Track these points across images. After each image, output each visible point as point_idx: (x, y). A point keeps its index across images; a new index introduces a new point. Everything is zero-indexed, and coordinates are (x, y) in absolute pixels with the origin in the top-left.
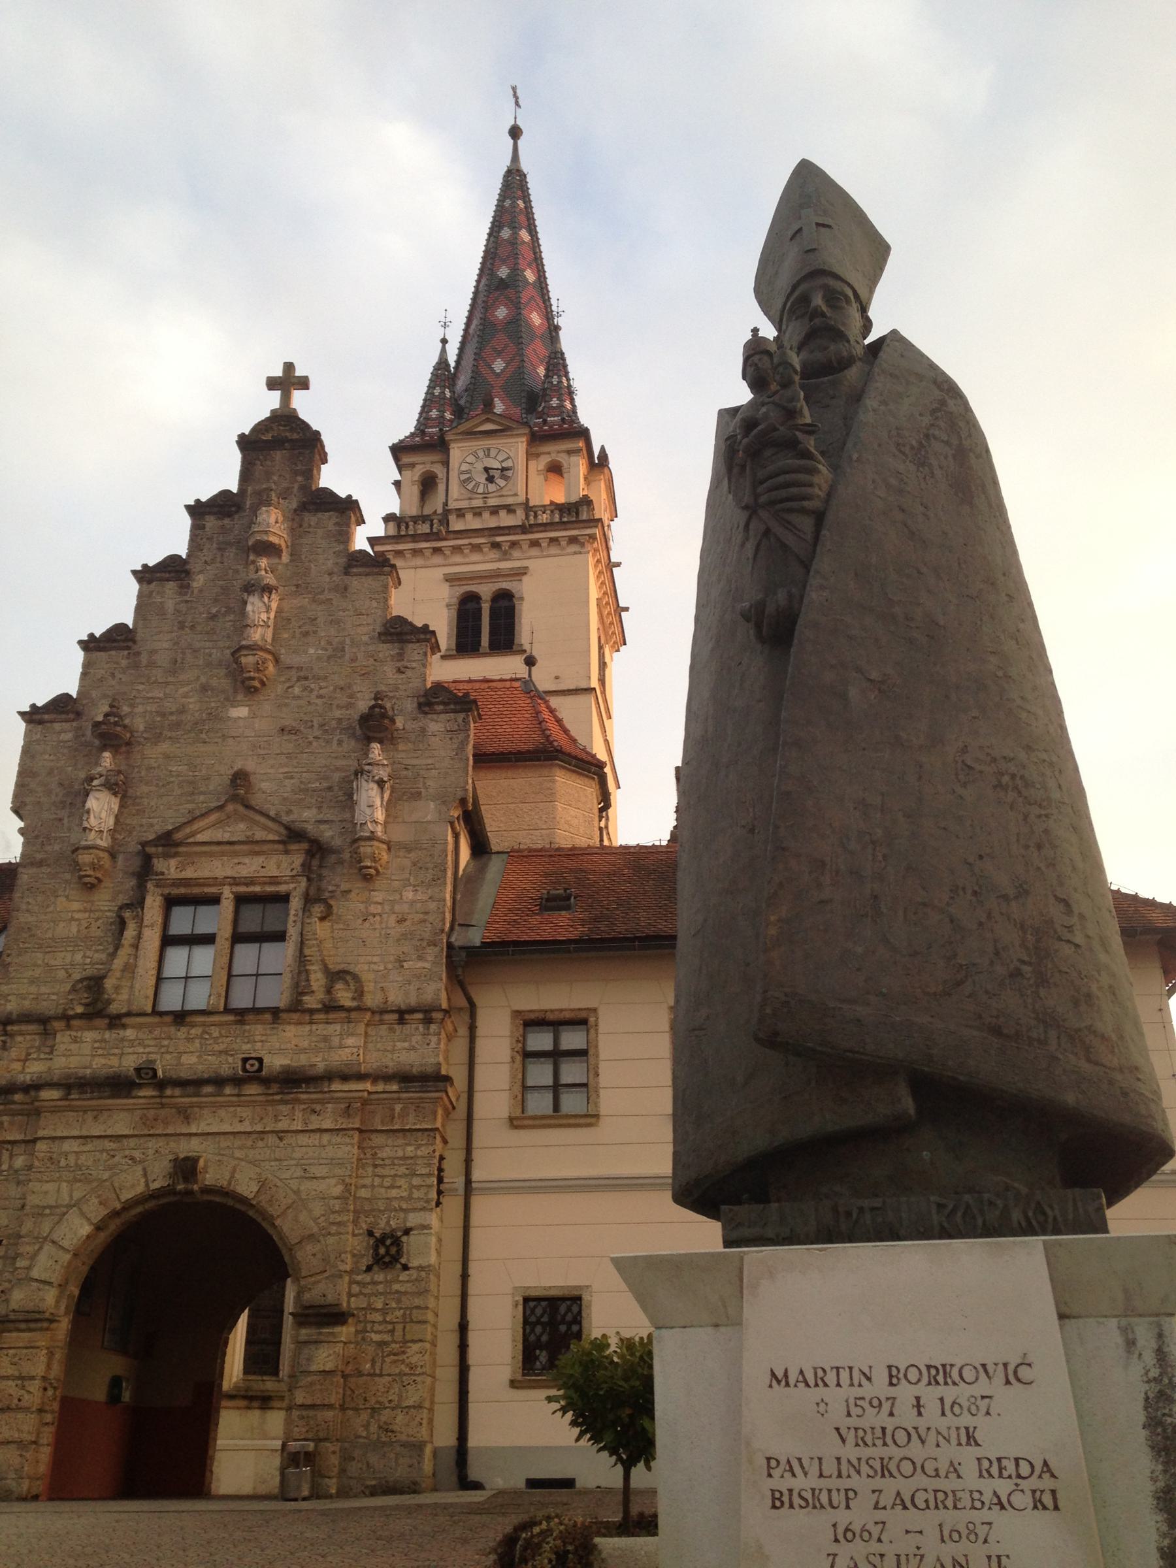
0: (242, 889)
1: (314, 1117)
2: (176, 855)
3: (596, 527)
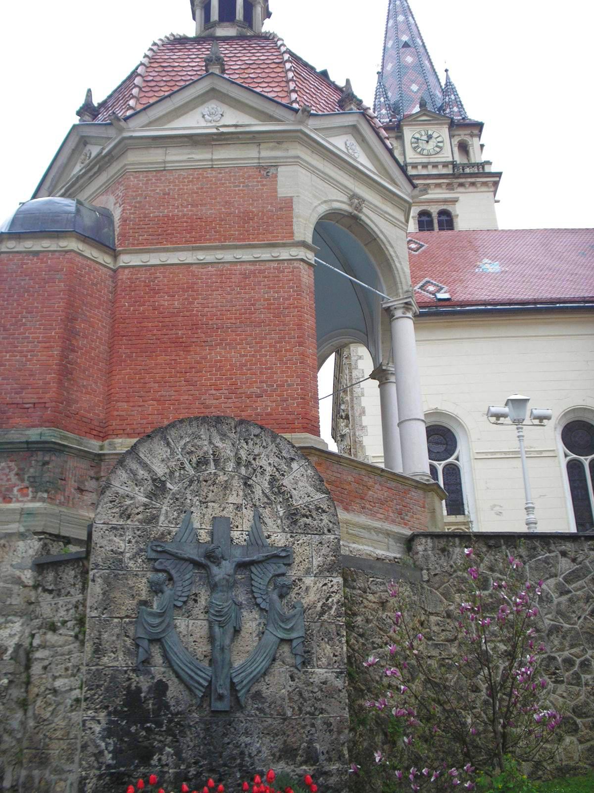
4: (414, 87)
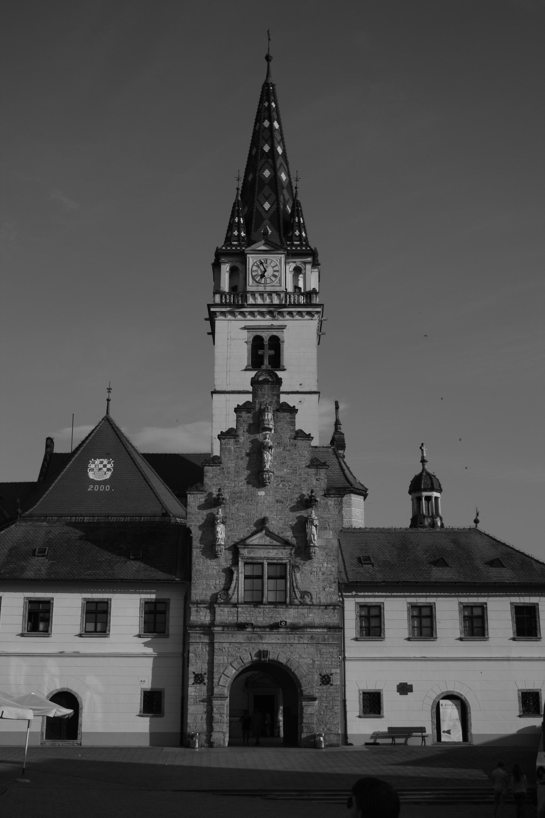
0: (270, 561)
1: (301, 639)
2: (248, 548)
3: (321, 307)
4: (267, 206)
